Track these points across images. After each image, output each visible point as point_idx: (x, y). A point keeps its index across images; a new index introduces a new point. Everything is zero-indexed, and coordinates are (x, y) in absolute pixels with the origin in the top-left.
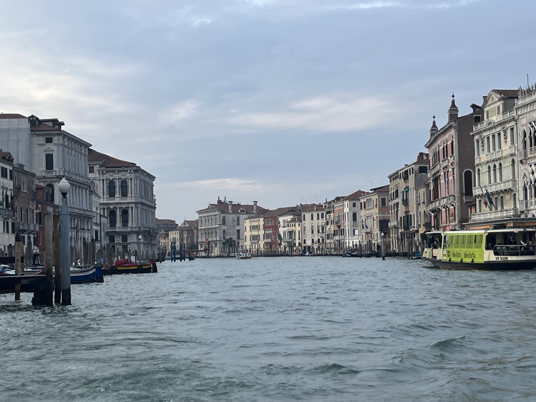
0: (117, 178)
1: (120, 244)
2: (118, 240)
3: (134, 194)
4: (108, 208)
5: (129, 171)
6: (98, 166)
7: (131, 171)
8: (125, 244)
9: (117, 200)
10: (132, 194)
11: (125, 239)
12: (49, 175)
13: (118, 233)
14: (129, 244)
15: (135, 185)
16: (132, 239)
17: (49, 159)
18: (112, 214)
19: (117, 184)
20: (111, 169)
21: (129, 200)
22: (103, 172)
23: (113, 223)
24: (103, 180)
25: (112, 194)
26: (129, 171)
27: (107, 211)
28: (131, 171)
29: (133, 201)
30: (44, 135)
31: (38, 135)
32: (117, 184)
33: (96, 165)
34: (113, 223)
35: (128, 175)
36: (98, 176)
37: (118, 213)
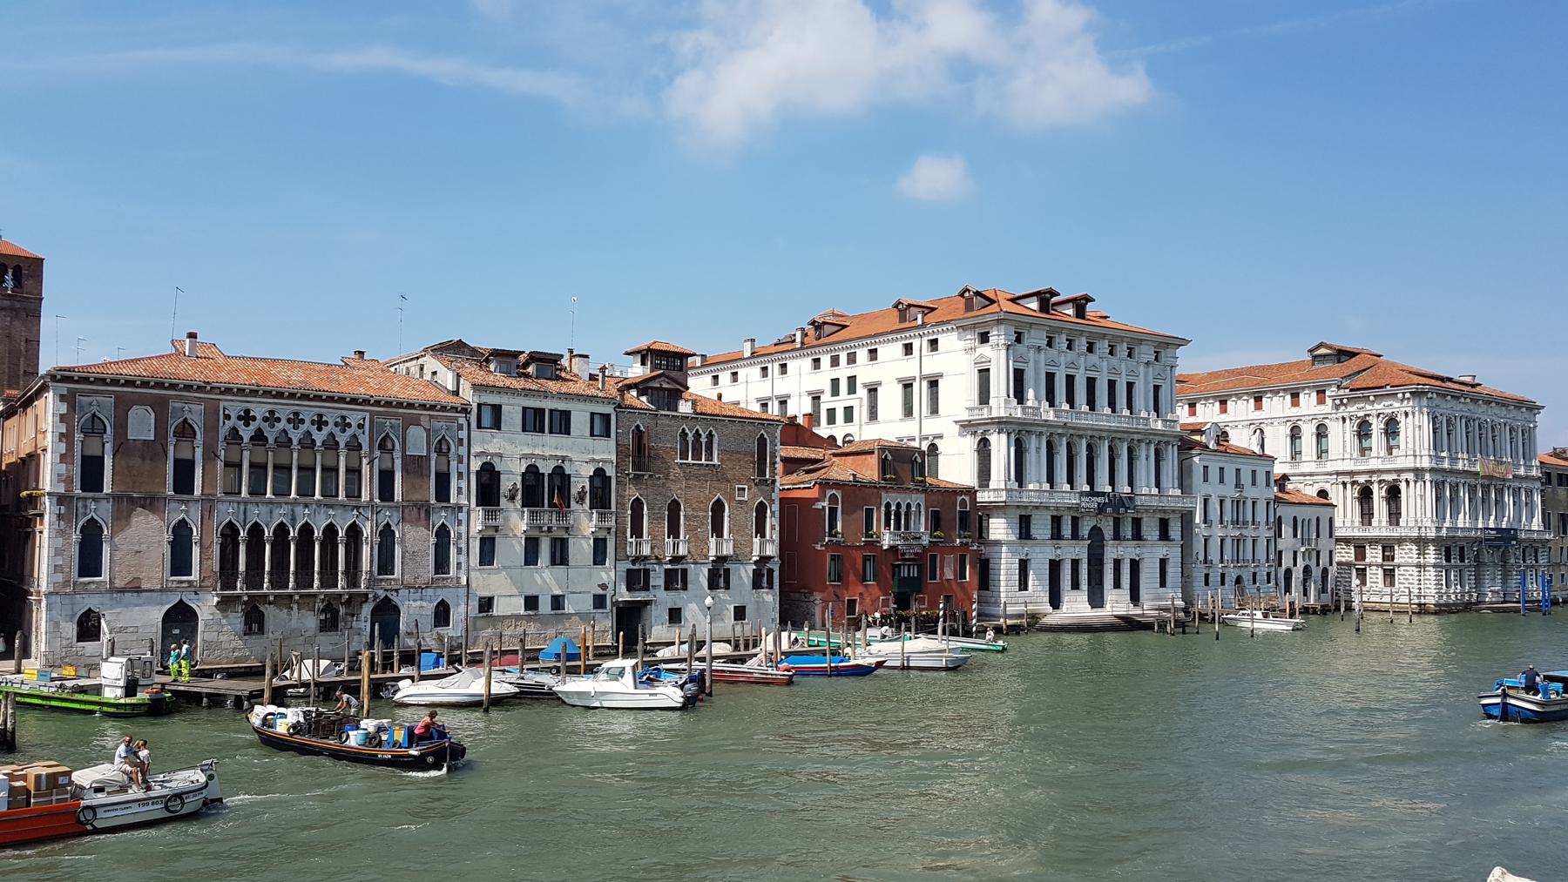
9: (1374, 464)
13: (1373, 541)
16: (1405, 555)
18: (1365, 494)
19: (1377, 426)
21: (1400, 463)
24: (1344, 419)
30: (974, 326)
31: (964, 328)
32: (1377, 426)
35: (1395, 407)
37: (1378, 494)
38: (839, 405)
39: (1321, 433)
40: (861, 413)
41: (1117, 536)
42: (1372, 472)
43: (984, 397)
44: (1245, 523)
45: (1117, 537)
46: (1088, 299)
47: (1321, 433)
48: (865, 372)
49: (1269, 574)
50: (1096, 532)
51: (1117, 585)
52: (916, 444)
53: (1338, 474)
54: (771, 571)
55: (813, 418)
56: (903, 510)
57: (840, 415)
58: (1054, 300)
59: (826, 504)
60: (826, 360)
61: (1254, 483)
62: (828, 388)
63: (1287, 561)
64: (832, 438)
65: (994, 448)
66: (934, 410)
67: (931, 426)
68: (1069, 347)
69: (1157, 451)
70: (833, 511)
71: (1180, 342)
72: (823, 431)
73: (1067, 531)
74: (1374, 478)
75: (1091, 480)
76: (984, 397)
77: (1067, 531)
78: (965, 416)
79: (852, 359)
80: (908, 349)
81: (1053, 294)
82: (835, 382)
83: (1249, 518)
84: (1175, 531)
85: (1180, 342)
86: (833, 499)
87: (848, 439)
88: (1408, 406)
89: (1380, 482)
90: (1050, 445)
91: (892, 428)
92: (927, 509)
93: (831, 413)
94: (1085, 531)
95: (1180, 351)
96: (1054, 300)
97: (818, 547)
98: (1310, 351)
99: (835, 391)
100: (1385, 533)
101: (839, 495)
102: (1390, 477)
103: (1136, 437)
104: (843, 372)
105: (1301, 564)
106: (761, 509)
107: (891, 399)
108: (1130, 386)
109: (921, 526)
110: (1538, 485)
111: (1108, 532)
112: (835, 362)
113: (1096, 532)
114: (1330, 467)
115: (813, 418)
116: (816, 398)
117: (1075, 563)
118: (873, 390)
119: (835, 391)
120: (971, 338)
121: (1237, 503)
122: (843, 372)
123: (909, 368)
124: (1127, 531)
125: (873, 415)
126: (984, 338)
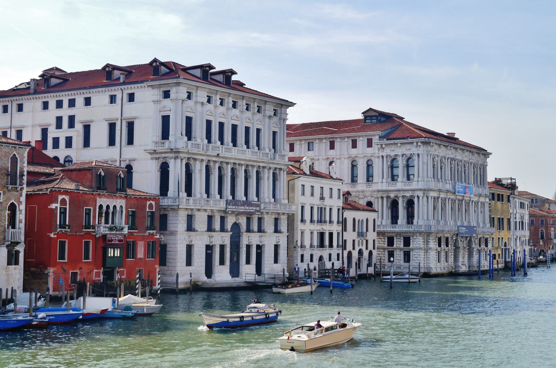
0: (400, 154)
1: (401, 249)
2: (399, 243)
3: (423, 177)
4: (388, 197)
5: (415, 144)
6: (377, 137)
7: (417, 143)
8: (406, 249)
9: (399, 185)
10: (419, 176)
11: (407, 242)
12: (160, 149)
13: (399, 234)
14: (413, 250)
15: (423, 163)
16: (417, 242)
17: (166, 120)
18: (394, 205)
19: (401, 163)
20: (392, 142)
21: (414, 185)
22: (382, 145)
23: (394, 219)
24: (383, 157)
25: (393, 178)
26: (415, 144)
27: (387, 201)
28: (417, 143)
29: (420, 187)
32: (401, 163)
33: (375, 135)
34: (394, 219)
36: (377, 151)
38: (62, 134)
39: (369, 166)
40: (78, 141)
41: (249, 230)
42: (399, 191)
43: (165, 135)
44: (325, 222)
45: (249, 230)
46: (233, 72)
47: (369, 166)
48: (81, 113)
49: (338, 255)
50: (236, 226)
51: (248, 262)
52: (118, 164)
53: (378, 191)
54: (17, 252)
55: (43, 143)
56: (111, 209)
57: (62, 143)
58: (211, 71)
59: (58, 205)
60: (52, 104)
61: (331, 197)
62: (54, 122)
63: (349, 247)
64: (56, 159)
65: (171, 169)
66: (130, 141)
67: (129, 153)
68: (221, 104)
69: (274, 174)
70: (63, 213)
71: (292, 104)
72: (50, 152)
73: (217, 225)
74: (402, 194)
75: (233, 193)
76: (165, 135)
77: (217, 225)
78: (151, 147)
79: (72, 103)
80: (113, 99)
81: (211, 67)
82: (59, 120)
83: (328, 219)
84: (283, 226)
85: (292, 104)
86: (63, 202)
87: (68, 160)
88: (422, 150)
89: (403, 197)
90: (208, 168)
91: (100, 153)
92: (126, 209)
93: (56, 141)
94: (229, 226)
95: (290, 110)
96: (211, 71)
97: (52, 235)
98: (363, 113)
99: (59, 125)
100: (405, 229)
101: (67, 198)
102: (408, 194)
103: (261, 165)
104: (65, 112)
105: (357, 248)
106: (13, 208)
107: (100, 134)
108: (258, 131)
109: (121, 221)
110: (487, 200)
111: (244, 227)
112: (59, 104)
113: (236, 226)
114: (375, 187)
115: (43, 143)
116: (45, 132)
117: (222, 247)
118: (87, 128)
119: (59, 125)
120: (156, 94)
121: (321, 210)
122: (65, 112)
123: (114, 112)
124: (255, 227)
125: (87, 143)
126: (167, 95)
